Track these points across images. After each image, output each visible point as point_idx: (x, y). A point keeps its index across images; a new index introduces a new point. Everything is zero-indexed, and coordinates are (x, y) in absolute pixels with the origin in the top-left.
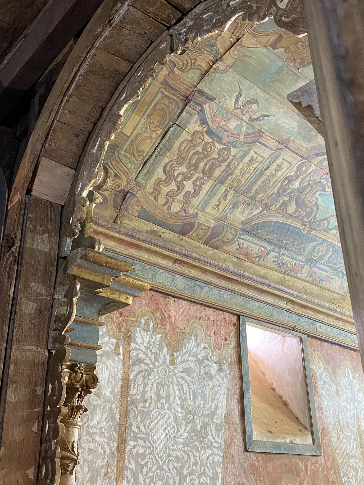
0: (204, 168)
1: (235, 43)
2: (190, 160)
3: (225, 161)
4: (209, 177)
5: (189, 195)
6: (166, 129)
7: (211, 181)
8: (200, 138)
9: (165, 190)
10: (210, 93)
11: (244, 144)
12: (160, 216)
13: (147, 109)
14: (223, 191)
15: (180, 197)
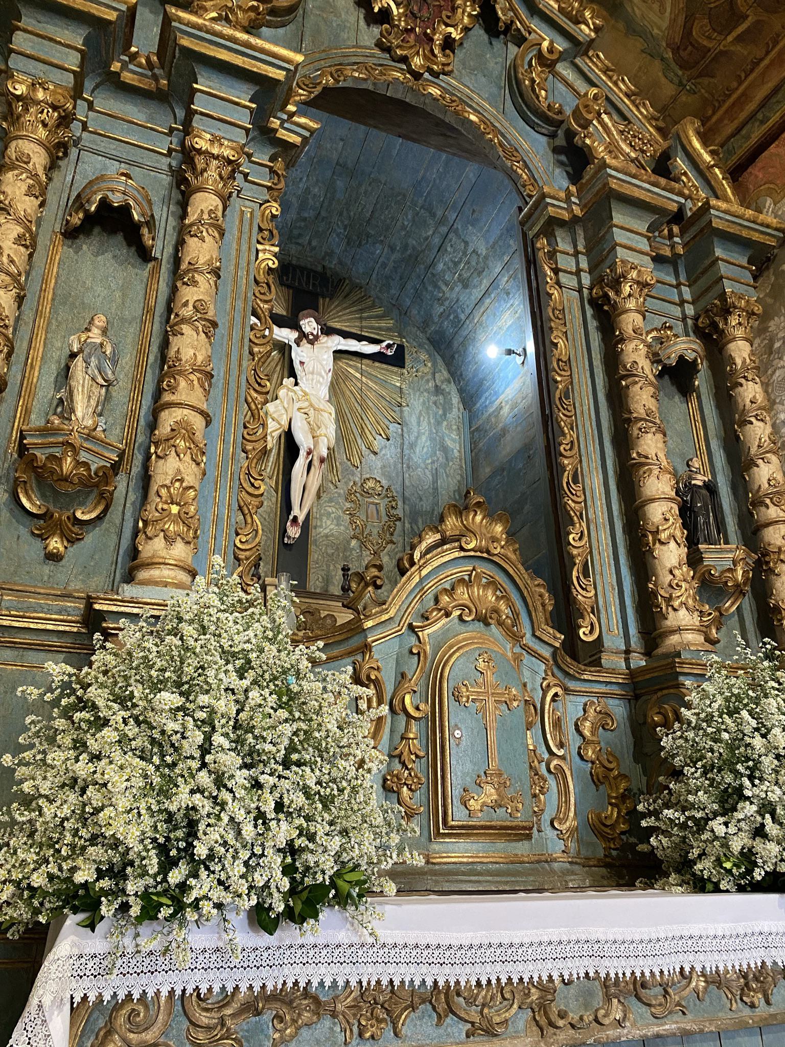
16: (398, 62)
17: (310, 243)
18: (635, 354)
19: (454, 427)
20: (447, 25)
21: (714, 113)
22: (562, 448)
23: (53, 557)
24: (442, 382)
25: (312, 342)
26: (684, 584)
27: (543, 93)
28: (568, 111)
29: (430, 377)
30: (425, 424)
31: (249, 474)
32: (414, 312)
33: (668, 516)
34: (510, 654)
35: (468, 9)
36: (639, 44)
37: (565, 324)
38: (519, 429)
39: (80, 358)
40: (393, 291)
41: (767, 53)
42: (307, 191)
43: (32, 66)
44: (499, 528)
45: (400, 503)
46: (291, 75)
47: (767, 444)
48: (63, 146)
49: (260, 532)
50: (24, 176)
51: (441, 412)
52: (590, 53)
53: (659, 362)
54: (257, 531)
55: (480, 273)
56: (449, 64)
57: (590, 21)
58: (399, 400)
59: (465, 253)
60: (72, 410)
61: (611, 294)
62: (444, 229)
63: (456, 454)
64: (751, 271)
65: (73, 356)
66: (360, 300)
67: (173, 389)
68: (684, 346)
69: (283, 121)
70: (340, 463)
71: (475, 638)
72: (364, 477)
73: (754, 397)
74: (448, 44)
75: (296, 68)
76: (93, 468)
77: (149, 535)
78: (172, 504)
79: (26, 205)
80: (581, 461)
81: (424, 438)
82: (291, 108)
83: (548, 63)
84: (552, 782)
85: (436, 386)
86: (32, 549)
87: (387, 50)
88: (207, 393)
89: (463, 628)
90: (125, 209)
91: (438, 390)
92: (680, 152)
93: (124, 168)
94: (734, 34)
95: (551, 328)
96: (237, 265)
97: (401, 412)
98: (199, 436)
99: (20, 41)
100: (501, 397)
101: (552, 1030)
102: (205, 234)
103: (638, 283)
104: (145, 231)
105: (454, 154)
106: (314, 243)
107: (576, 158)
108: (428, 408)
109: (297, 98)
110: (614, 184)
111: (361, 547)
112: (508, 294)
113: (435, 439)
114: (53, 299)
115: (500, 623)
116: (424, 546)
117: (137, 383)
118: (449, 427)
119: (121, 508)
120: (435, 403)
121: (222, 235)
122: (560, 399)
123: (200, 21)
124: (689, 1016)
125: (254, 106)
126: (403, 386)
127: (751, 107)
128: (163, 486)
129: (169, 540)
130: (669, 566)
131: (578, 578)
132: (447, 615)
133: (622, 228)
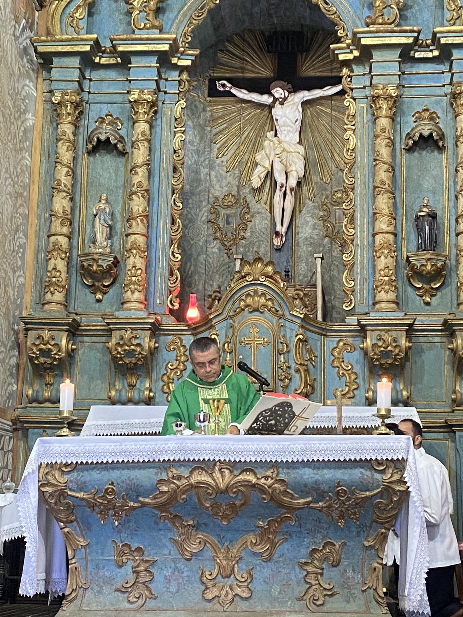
17: (285, 15)
23: (99, 301)
25: (282, 103)
26: (386, 278)
33: (382, 242)
43: (62, 85)
53: (410, 138)
65: (95, 216)
67: (131, 226)
70: (316, 184)
72: (334, 190)
82: (182, 49)
84: (297, 375)
86: (91, 298)
99: (55, 74)
110: (363, 42)
111: (331, 243)
115: (269, 310)
116: (234, 280)
128: (129, 270)
129: (133, 292)
130: (379, 268)
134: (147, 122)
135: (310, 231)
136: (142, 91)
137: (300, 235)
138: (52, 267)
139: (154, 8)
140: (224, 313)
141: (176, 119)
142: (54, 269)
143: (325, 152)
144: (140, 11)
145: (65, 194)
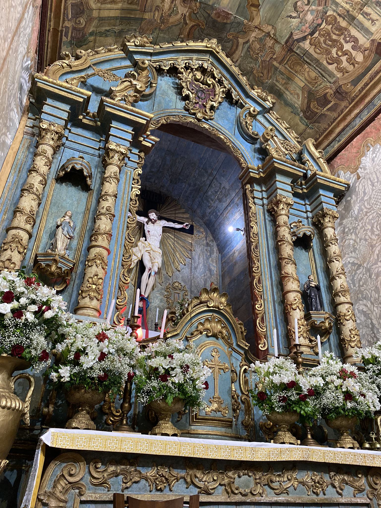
0: (338, 35)
1: (258, 28)
2: (328, 46)
3: (336, 18)
4: (346, 29)
5: (355, 46)
6: (305, 62)
7: (349, 28)
8: (315, 40)
9: (345, 64)
10: (287, 36)
11: (325, 5)
12: (361, 71)
13: (292, 73)
14: (362, 16)
15: (354, 53)
16: (192, 115)
17: (154, 182)
18: (284, 232)
19: (215, 261)
20: (212, 101)
21: (320, 137)
22: (254, 269)
24: (210, 241)
25: (153, 223)
27: (251, 127)
28: (261, 135)
29: (204, 239)
30: (202, 259)
31: (124, 275)
32: (198, 211)
33: (296, 298)
34: (226, 351)
35: (221, 95)
36: (290, 110)
37: (256, 219)
38: (242, 262)
39: (60, 228)
40: (189, 202)
41: (339, 116)
42: (154, 161)
44: (223, 300)
45: (189, 293)
46: (148, 122)
47: (340, 271)
48: (59, 147)
49: (127, 298)
50: (44, 159)
51: (209, 254)
52: (271, 112)
53: (295, 235)
54: (126, 298)
55: (226, 197)
56: (212, 116)
57: (270, 100)
58: (190, 248)
59: (220, 188)
60: (56, 248)
61: (275, 208)
62: (211, 178)
63: (215, 272)
64: (335, 200)
65: (58, 227)
66: (175, 205)
67: (96, 240)
68: (306, 229)
69: (144, 138)
71: (211, 343)
72: (174, 281)
73: (335, 251)
74: (212, 108)
75: (151, 119)
76: (63, 269)
77: (83, 296)
78: (93, 284)
79: (43, 169)
80: (261, 275)
81: (201, 265)
82: (148, 133)
83: (253, 116)
85: (207, 243)
87: (187, 110)
88: (109, 241)
89: (208, 339)
90: (81, 171)
91: (208, 245)
92: (306, 152)
93: (81, 155)
94: (327, 108)
95: (251, 220)
96: (124, 193)
97: (191, 253)
98: (105, 258)
99: (46, 108)
100: (235, 248)
101: (232, 495)
102: (112, 181)
103: (286, 204)
104: (88, 179)
105: (215, 149)
106: (156, 182)
107: (263, 153)
108: (203, 252)
109: (151, 128)
110: (276, 165)
112: (238, 205)
113: (206, 266)
114: (50, 204)
115: (223, 338)
117: (81, 237)
118: (212, 261)
119: (72, 286)
120: (206, 250)
121: (118, 181)
122: (254, 249)
123: (115, 102)
124: (290, 495)
125: (134, 133)
126: (193, 242)
127: (334, 135)
128: (90, 278)
129: (91, 299)
131: (259, 323)
132: (201, 333)
133: (280, 182)
134: (118, 166)
135: (158, 303)
136: (118, 145)
137: (152, 304)
138: (6, 258)
139: (132, 101)
140: (181, 334)
141: (134, 179)
142: (9, 260)
143: (170, 258)
144: (122, 100)
145: (35, 197)
